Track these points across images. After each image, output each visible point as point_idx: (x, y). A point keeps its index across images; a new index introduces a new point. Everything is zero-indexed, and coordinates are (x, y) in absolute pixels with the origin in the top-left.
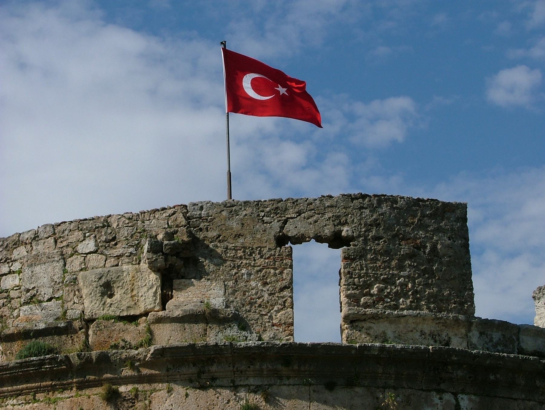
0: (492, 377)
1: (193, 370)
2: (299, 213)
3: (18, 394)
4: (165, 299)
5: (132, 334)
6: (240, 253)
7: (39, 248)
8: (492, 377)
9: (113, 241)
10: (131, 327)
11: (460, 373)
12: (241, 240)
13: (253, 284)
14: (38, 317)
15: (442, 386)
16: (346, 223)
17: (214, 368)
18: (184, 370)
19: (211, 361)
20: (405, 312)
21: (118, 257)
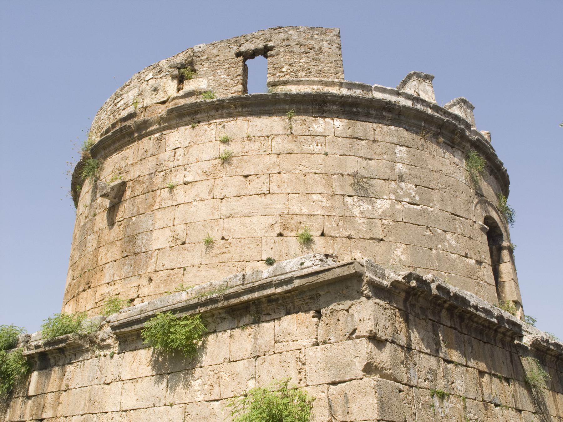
0: (355, 110)
1: (188, 118)
2: (247, 41)
3: (115, 152)
4: (179, 90)
6: (217, 64)
8: (355, 110)
9: (160, 72)
10: (161, 106)
11: (334, 107)
12: (218, 58)
13: (222, 76)
15: (325, 115)
16: (270, 41)
17: (198, 116)
18: (184, 119)
19: (196, 112)
20: (302, 79)
21: (161, 78)
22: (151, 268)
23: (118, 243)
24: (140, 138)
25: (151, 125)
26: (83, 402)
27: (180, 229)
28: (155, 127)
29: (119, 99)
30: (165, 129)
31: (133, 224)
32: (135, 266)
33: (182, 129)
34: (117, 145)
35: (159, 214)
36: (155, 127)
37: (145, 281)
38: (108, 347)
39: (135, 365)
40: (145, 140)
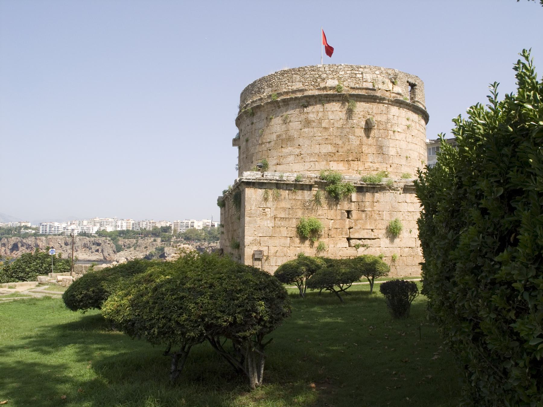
3: (364, 102)
5: (388, 94)
7: (365, 70)
14: (370, 86)
22: (391, 162)
23: (375, 147)
24: (379, 103)
25: (385, 100)
26: (388, 207)
27: (399, 150)
28: (387, 102)
29: (357, 72)
30: (390, 104)
31: (380, 141)
32: (384, 159)
33: (395, 107)
34: (366, 100)
35: (391, 140)
36: (387, 102)
37: (389, 166)
38: (399, 190)
39: (412, 198)
40: (381, 105)
